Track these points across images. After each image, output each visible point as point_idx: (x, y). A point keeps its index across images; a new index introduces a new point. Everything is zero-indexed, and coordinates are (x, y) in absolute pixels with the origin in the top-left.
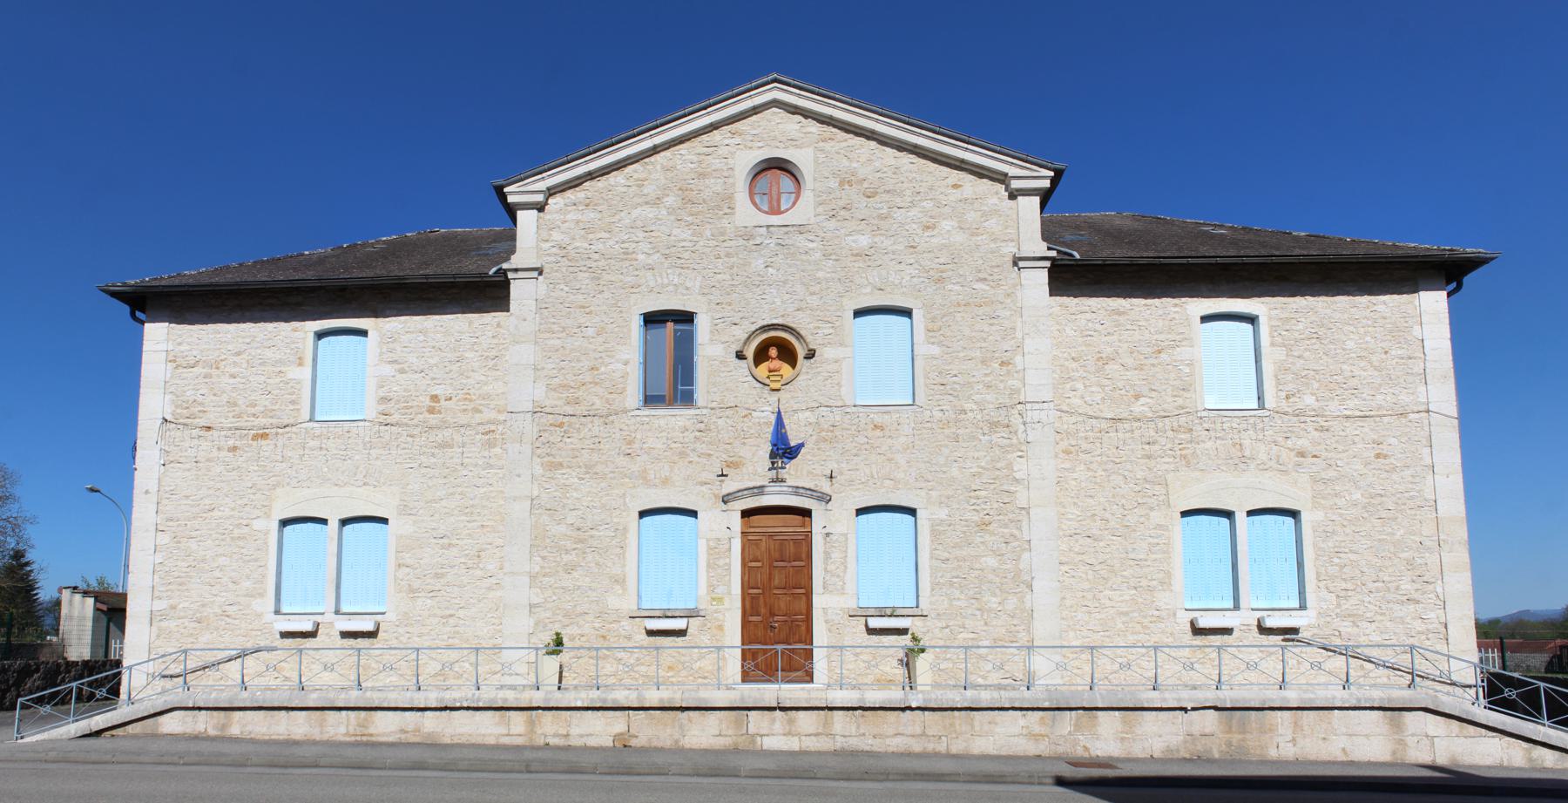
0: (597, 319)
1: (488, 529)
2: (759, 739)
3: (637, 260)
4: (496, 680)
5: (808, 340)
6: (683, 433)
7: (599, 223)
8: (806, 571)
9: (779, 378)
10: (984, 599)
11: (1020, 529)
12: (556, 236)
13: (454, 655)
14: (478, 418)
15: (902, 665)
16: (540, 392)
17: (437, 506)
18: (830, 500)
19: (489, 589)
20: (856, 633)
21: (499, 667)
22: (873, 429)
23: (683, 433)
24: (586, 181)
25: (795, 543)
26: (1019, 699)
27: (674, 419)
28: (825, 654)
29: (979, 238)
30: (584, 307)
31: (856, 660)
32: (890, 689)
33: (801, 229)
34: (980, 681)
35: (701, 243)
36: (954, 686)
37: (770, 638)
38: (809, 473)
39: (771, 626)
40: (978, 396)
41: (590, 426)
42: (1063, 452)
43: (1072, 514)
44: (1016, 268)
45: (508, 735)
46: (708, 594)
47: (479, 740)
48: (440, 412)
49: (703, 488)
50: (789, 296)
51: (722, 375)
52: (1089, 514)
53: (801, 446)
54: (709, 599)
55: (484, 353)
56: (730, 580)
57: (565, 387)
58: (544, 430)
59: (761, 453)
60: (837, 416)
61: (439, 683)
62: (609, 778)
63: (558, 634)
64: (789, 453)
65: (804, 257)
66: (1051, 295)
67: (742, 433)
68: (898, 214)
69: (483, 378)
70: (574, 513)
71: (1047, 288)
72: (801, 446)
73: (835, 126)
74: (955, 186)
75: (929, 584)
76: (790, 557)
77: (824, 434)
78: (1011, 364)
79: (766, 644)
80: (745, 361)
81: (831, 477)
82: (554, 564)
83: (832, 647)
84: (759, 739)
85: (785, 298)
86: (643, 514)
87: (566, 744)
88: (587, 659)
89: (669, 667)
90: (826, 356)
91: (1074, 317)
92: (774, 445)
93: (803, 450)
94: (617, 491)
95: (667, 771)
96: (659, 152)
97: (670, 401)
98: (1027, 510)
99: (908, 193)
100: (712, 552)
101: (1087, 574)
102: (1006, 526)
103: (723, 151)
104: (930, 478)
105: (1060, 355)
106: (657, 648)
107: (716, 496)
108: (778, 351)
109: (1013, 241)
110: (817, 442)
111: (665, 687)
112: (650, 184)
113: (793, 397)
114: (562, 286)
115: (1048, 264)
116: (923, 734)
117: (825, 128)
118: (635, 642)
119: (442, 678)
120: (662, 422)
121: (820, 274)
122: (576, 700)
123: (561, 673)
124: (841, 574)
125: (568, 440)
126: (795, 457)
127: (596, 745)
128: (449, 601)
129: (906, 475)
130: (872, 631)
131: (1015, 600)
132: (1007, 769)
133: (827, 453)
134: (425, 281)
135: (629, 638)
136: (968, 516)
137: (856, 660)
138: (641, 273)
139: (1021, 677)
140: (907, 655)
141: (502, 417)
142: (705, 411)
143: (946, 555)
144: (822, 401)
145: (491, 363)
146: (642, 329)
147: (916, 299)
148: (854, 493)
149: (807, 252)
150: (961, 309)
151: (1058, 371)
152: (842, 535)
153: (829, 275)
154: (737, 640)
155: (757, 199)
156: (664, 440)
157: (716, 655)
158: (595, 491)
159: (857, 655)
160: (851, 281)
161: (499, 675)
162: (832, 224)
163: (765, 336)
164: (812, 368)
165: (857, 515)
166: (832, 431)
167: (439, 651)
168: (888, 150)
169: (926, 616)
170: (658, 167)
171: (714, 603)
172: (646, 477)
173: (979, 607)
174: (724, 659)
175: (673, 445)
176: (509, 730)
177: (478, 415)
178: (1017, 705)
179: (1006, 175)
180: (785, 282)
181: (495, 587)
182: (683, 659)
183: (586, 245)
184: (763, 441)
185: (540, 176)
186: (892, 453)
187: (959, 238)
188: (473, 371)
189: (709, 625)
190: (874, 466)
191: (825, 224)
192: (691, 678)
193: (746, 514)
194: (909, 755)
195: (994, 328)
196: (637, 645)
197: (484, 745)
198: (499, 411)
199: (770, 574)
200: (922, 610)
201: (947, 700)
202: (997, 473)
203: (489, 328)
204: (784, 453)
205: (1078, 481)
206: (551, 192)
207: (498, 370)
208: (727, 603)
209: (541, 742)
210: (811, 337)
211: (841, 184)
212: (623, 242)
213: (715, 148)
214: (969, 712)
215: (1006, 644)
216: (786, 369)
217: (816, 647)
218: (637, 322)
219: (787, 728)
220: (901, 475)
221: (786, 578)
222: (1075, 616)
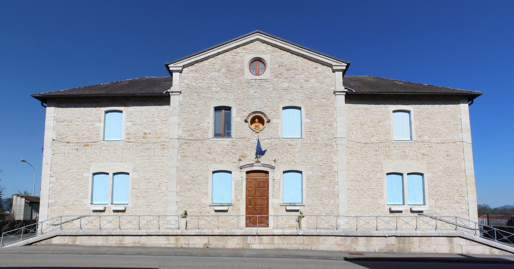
0: (199, 108)
1: (163, 177)
2: (251, 245)
3: (212, 89)
4: (165, 226)
5: (268, 117)
6: (227, 146)
7: (200, 77)
9: (258, 129)
10: (323, 200)
11: (335, 178)
12: (186, 81)
13: (151, 218)
14: (159, 140)
16: (180, 132)
17: (146, 169)
18: (275, 168)
19: (163, 196)
20: (282, 211)
21: (166, 222)
22: (288, 146)
23: (227, 146)
24: (196, 63)
25: (263, 182)
26: (334, 232)
29: (323, 85)
30: (195, 105)
31: (282, 220)
32: (293, 229)
33: (266, 80)
34: (322, 227)
35: (233, 85)
36: (314, 228)
38: (268, 159)
40: (322, 136)
41: (197, 143)
42: (350, 153)
43: (352, 174)
44: (335, 95)
45: (169, 244)
46: (235, 198)
47: (160, 246)
48: (147, 138)
49: (234, 164)
51: (240, 127)
52: (357, 174)
53: (266, 151)
55: (162, 119)
56: (242, 194)
57: (189, 130)
58: (182, 145)
59: (253, 153)
60: (277, 141)
61: (146, 227)
62: (202, 257)
63: (185, 211)
64: (262, 153)
65: (267, 90)
66: (346, 103)
68: (297, 76)
69: (161, 127)
70: (191, 172)
71: (344, 101)
72: (266, 151)
73: (277, 48)
74: (316, 68)
75: (306, 195)
77: (273, 147)
78: (332, 125)
79: (254, 215)
81: (275, 161)
82: (184, 188)
83: (275, 216)
84: (251, 245)
86: (214, 172)
87: (188, 247)
88: (195, 219)
89: (222, 222)
91: (353, 110)
92: (257, 151)
94: (205, 165)
95: (221, 255)
96: (220, 54)
97: (223, 136)
98: (337, 172)
99: (300, 70)
101: (356, 193)
102: (330, 177)
103: (241, 54)
104: (307, 162)
105: (349, 123)
106: (218, 216)
107: (238, 167)
108: (258, 120)
109: (334, 86)
111: (220, 228)
112: (216, 65)
113: (263, 135)
114: (188, 98)
115: (345, 93)
116: (303, 244)
117: (274, 48)
118: (211, 214)
119: (147, 226)
120: (220, 142)
121: (272, 95)
122: (191, 232)
123: (186, 224)
124: (278, 192)
125: (189, 148)
127: (198, 247)
128: (149, 200)
129: (299, 161)
130: (287, 211)
131: (333, 201)
132: (330, 255)
133: (274, 153)
134: (142, 95)
135: (209, 213)
136: (318, 174)
137: (282, 220)
138: (214, 94)
139: (335, 226)
140: (299, 218)
141: (167, 140)
143: (311, 186)
145: (164, 122)
147: (302, 104)
149: (268, 88)
150: (317, 107)
151: (348, 128)
153: (275, 96)
154: (244, 213)
155: (252, 71)
156: (221, 148)
157: (237, 218)
158: (198, 164)
159: (282, 218)
161: (166, 224)
162: (276, 79)
163: (254, 115)
164: (269, 126)
165: (283, 173)
166: (275, 146)
167: (146, 217)
168: (294, 56)
169: (305, 206)
170: (220, 59)
171: (237, 201)
173: (322, 203)
174: (240, 219)
175: (224, 150)
176: (169, 242)
177: (159, 139)
178: (333, 235)
179: (332, 65)
180: (261, 98)
181: (165, 196)
182: (226, 219)
183: (196, 84)
185: (180, 62)
187: (317, 85)
188: (158, 125)
189: (235, 208)
190: (288, 158)
191: (273, 79)
192: (229, 226)
193: (248, 172)
194: (299, 250)
195: (327, 114)
197: (161, 247)
198: (166, 138)
200: (303, 204)
201: (311, 233)
202: (328, 160)
203: (163, 111)
204: (260, 153)
205: (354, 163)
206: (184, 67)
207: (166, 125)
208: (241, 201)
209: (180, 246)
210: (269, 116)
211: (279, 66)
212: (208, 84)
213: (238, 54)
214: (318, 236)
215: (330, 215)
216: (261, 126)
218: (212, 110)
219: (260, 242)
221: (260, 193)
222: (353, 207)
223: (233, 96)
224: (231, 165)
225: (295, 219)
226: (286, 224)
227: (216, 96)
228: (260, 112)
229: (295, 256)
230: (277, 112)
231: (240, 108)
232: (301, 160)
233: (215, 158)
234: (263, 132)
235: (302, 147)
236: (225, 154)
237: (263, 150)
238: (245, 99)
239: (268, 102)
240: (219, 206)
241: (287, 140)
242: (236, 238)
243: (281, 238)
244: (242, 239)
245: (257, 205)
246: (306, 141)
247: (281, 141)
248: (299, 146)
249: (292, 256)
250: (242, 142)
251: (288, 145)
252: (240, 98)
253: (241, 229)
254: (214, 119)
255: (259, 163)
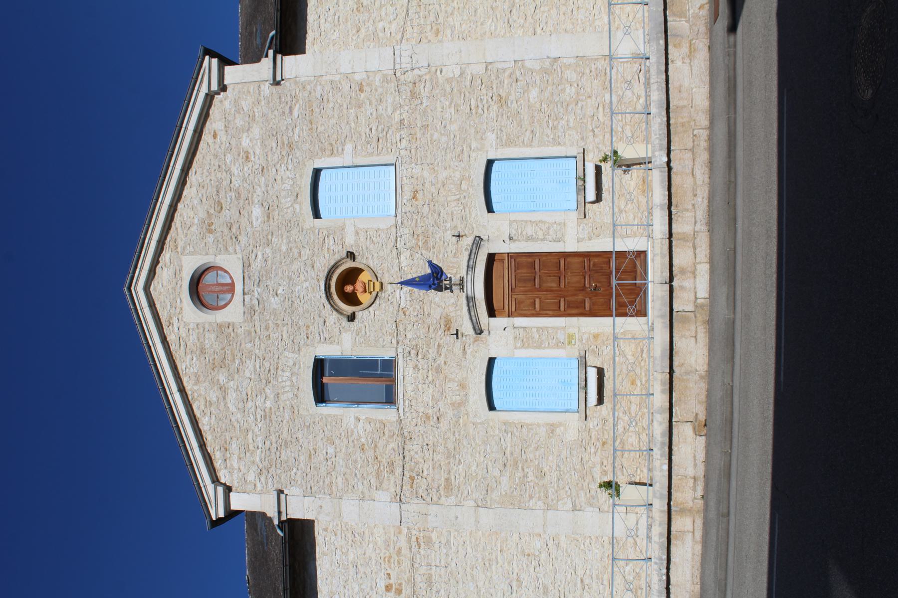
0: (320, 444)
1: (504, 545)
2: (699, 301)
3: (271, 408)
4: (642, 542)
5: (339, 258)
6: (419, 370)
7: (240, 439)
8: (544, 258)
9: (371, 283)
10: (568, 99)
11: (504, 70)
12: (251, 477)
13: (618, 579)
14: (406, 551)
15: (629, 170)
16: (383, 496)
17: (483, 591)
18: (479, 237)
19: (558, 547)
20: (600, 212)
21: (630, 540)
22: (417, 200)
23: (419, 370)
24: (207, 450)
25: (518, 270)
26: (658, 66)
27: (407, 378)
28: (620, 239)
29: (257, 114)
30: (310, 455)
31: (625, 211)
32: (651, 181)
33: (246, 265)
34: (642, 101)
35: (257, 351)
36: (647, 124)
37: (607, 290)
38: (455, 256)
39: (595, 289)
40: (389, 109)
41: (412, 453)
42: (437, 36)
43: (491, 26)
44: (282, 82)
45: (693, 533)
46: (564, 348)
47: (698, 559)
48: (400, 584)
49: (469, 351)
50: (301, 276)
51: (368, 334)
52: (491, 12)
53: (430, 263)
55: (350, 544)
57: (378, 473)
58: (416, 493)
60: (405, 231)
61: (644, 594)
62: (735, 441)
63: (601, 486)
64: (438, 274)
65: (269, 262)
66: (304, 52)
68: (236, 183)
69: (371, 546)
70: (490, 469)
71: (299, 57)
72: (430, 263)
73: (165, 238)
74: (215, 136)
75: (555, 148)
76: (532, 273)
77: (420, 243)
78: (361, 84)
79: (612, 294)
80: (356, 313)
81: (459, 236)
82: (536, 488)
83: (613, 233)
84: (699, 301)
86: (492, 407)
87: (702, 479)
88: (623, 460)
89: (632, 384)
90: (352, 242)
91: (323, 33)
92: (430, 288)
93: (435, 262)
94: (471, 431)
95: (729, 387)
96: (184, 387)
97: (391, 381)
98: (487, 65)
99: (219, 175)
101: (544, 12)
102: (502, 82)
103: (183, 333)
104: (460, 148)
105: (355, 42)
106: (615, 395)
107: (475, 341)
108: (348, 284)
109: (259, 87)
110: (427, 249)
112: (209, 395)
114: (293, 473)
115: (279, 56)
116: (692, 150)
117: (166, 246)
118: (609, 414)
119: (639, 591)
120: (410, 388)
121: (284, 248)
122: (661, 470)
123: (636, 484)
124: (547, 225)
125: (425, 473)
126: (441, 269)
127: (704, 452)
128: (569, 583)
129: (457, 170)
130: (599, 198)
131: (568, 72)
132: (722, 76)
134: (289, 591)
135: (605, 421)
136: (493, 115)
137: (625, 211)
138: (282, 405)
139: (637, 65)
140: (620, 166)
141: (405, 531)
142: (400, 350)
143: (528, 133)
145: (358, 538)
147: (305, 165)
148: (473, 216)
149: (266, 260)
150: (314, 126)
151: (368, 43)
152: (511, 225)
153: (285, 241)
154: (608, 321)
155: (222, 303)
156: (425, 386)
157: (622, 340)
158: (470, 450)
159: (621, 211)
160: (290, 221)
161: (637, 539)
162: (243, 239)
163: (335, 296)
164: (363, 255)
165: (494, 212)
167: (614, 593)
168: (185, 193)
169: (584, 149)
170: (196, 388)
171: (573, 342)
172: (459, 403)
173: (574, 103)
175: (430, 378)
176: (688, 532)
177: (403, 552)
178: (663, 68)
179: (207, 95)
180: (290, 278)
181: (557, 542)
182: (624, 371)
183: (259, 451)
184: (426, 297)
185: (203, 489)
186: (438, 183)
187: (256, 131)
188: (365, 554)
189: (593, 347)
191: (243, 245)
192: (642, 364)
193: (492, 313)
194: (711, 163)
195: (331, 99)
196: (611, 413)
197: (702, 554)
198: (400, 533)
199: (547, 291)
200: (578, 153)
201: (660, 130)
202: (455, 90)
203: (328, 539)
204: (438, 279)
205: (462, 22)
206: (215, 480)
207: (364, 532)
208: (571, 331)
209: (700, 503)
211: (210, 231)
212: (256, 419)
213: (181, 339)
214: (670, 110)
215: (608, 78)
216: (364, 277)
217: (614, 248)
218: (324, 409)
219: (689, 275)
220: (457, 174)
221: (550, 276)
222: (582, 20)
223: (286, 353)
224: (472, 360)
225: (623, 176)
227: (286, 398)
228: (326, 281)
229: (730, 170)
231: (317, 335)
232: (456, 164)
233: (453, 404)
235: (419, 163)
237: (429, 271)
238: (292, 322)
239: (300, 259)
240: (586, 393)
241: (400, 205)
242: (679, 342)
243: (679, 213)
244: (680, 325)
246: (403, 152)
247: (405, 221)
248: (417, 171)
249: (730, 181)
250: (408, 329)
251: (414, 201)
252: (291, 334)
253: (653, 330)
254: (346, 405)
255: (465, 280)
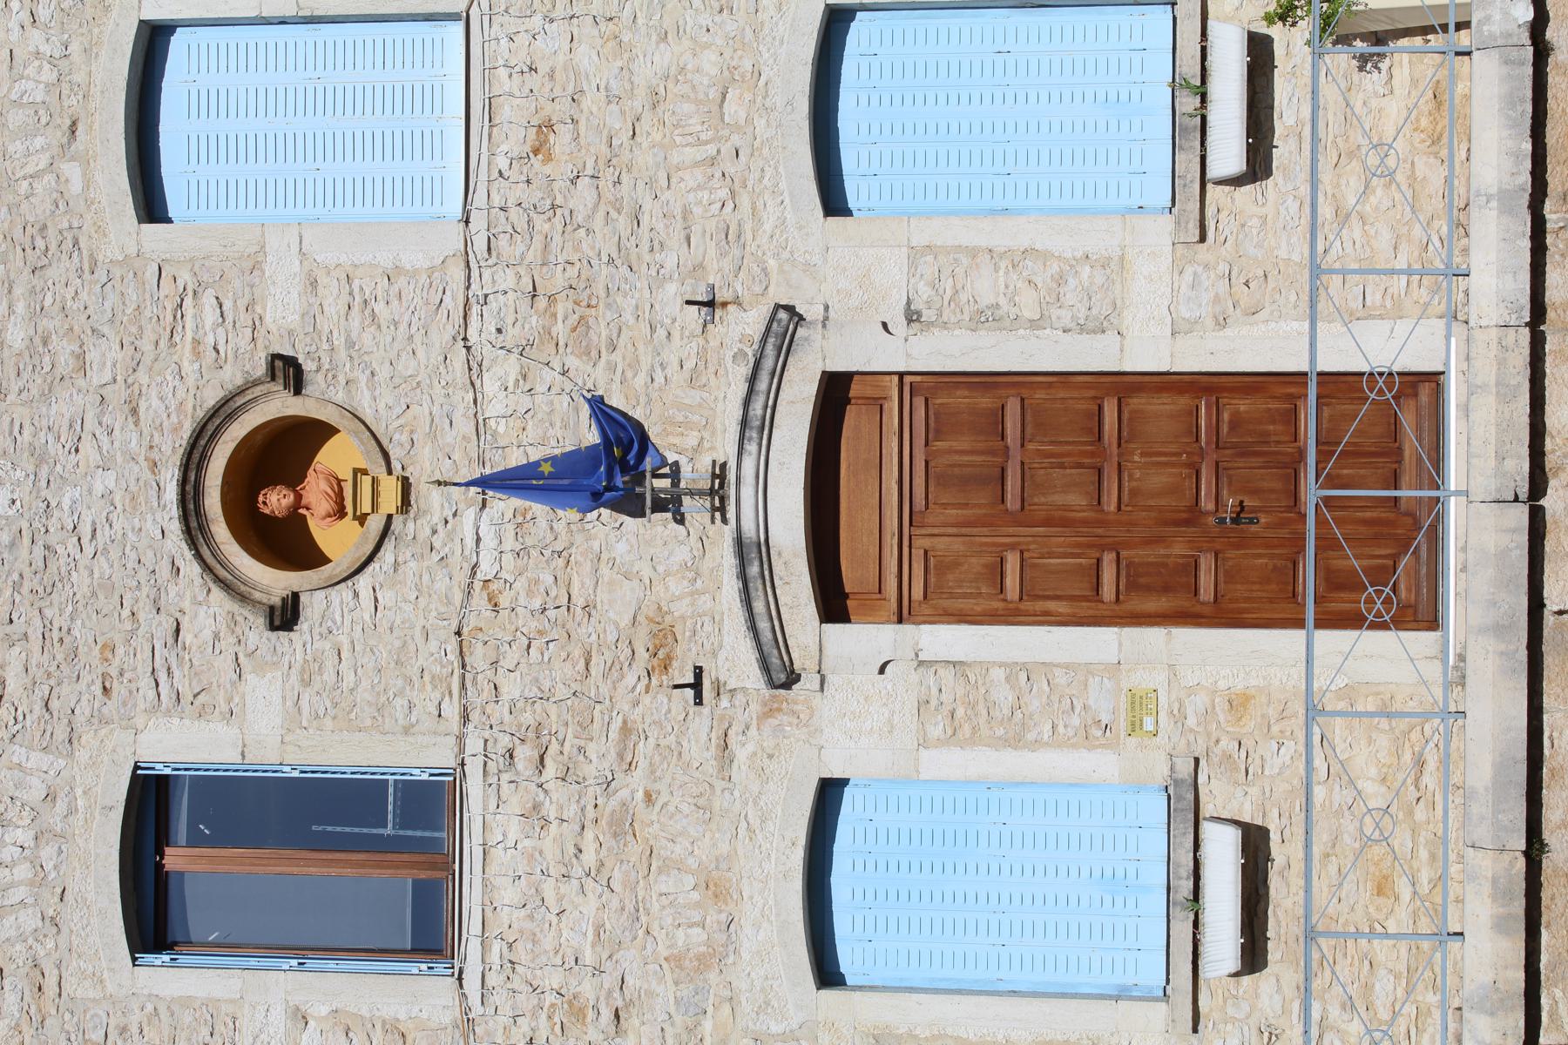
5: (239, 381)
8: (1040, 395)
9: (366, 482)
15: (1382, 56)
18: (790, 309)
20: (1264, 219)
22: (549, 158)
27: (497, 854)
28: (1337, 327)
32: (1468, 98)
37: (1281, 524)
39: (1236, 520)
49: (741, 754)
50: (87, 446)
51: (349, 679)
53: (600, 409)
54: (1133, 741)
64: (626, 451)
67: (551, 613)
72: (600, 409)
76: (992, 452)
77: (560, 330)
79: (1302, 538)
80: (303, 598)
81: (711, 304)
85: (94, 458)
86: (827, 973)
89: (1380, 891)
90: (293, 319)
92: (597, 499)
93: (616, 401)
97: (433, 866)
100: (967, 729)
106: (1310, 935)
107: (769, 712)
108: (272, 482)
110: (589, 353)
111: (1452, 909)
118: (1285, 1011)
120: (508, 894)
124: (1054, 268)
126: (638, 426)
129: (707, 46)
130: (1258, 165)
133: (628, 317)
140: (1344, 40)
142: (474, 745)
144: (447, 337)
146: (182, 959)
148: (768, 227)
152: (913, 263)
153: (20, 308)
154: (1284, 643)
157: (1338, 720)
160: (44, 227)
163: (220, 531)
164: (334, 367)
165: (847, 212)
166: (551, 298)
171: (1149, 724)
172: (700, 958)
174: (1348, 692)
175: (589, 858)
180: (40, 457)
182: (1349, 841)
184: (579, 539)
186: (632, 94)
190: (675, 158)
192: (1420, 813)
196: (1296, 1006)
199: (1047, 522)
204: (625, 469)
208: (1143, 680)
210: (228, 368)
216: (337, 457)
217: (1313, 360)
220: (709, 62)
221: (1062, 466)
224: (755, 788)
225: (1356, 76)
226: (1412, 177)
227: (13, 933)
228: (185, 468)
230: (185, 277)
231: (146, 682)
233: (676, 960)
234: (404, 438)
235: (559, 12)
236: (635, 850)
237: (592, 437)
238: (47, 628)
239: (81, 382)
240: (1196, 924)
241: (483, 176)
245: (1187, 501)
247: (502, 243)
248: (552, 45)
250: (508, 662)
251: (536, 161)
252: (40, 674)
253: (1462, 681)
254: (253, 962)
